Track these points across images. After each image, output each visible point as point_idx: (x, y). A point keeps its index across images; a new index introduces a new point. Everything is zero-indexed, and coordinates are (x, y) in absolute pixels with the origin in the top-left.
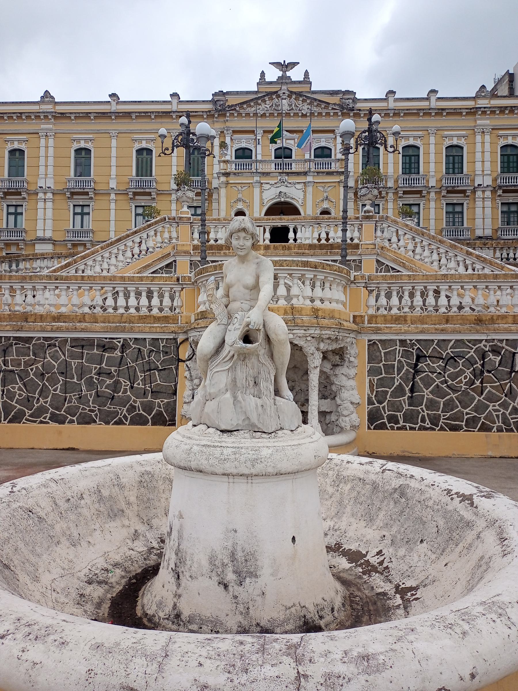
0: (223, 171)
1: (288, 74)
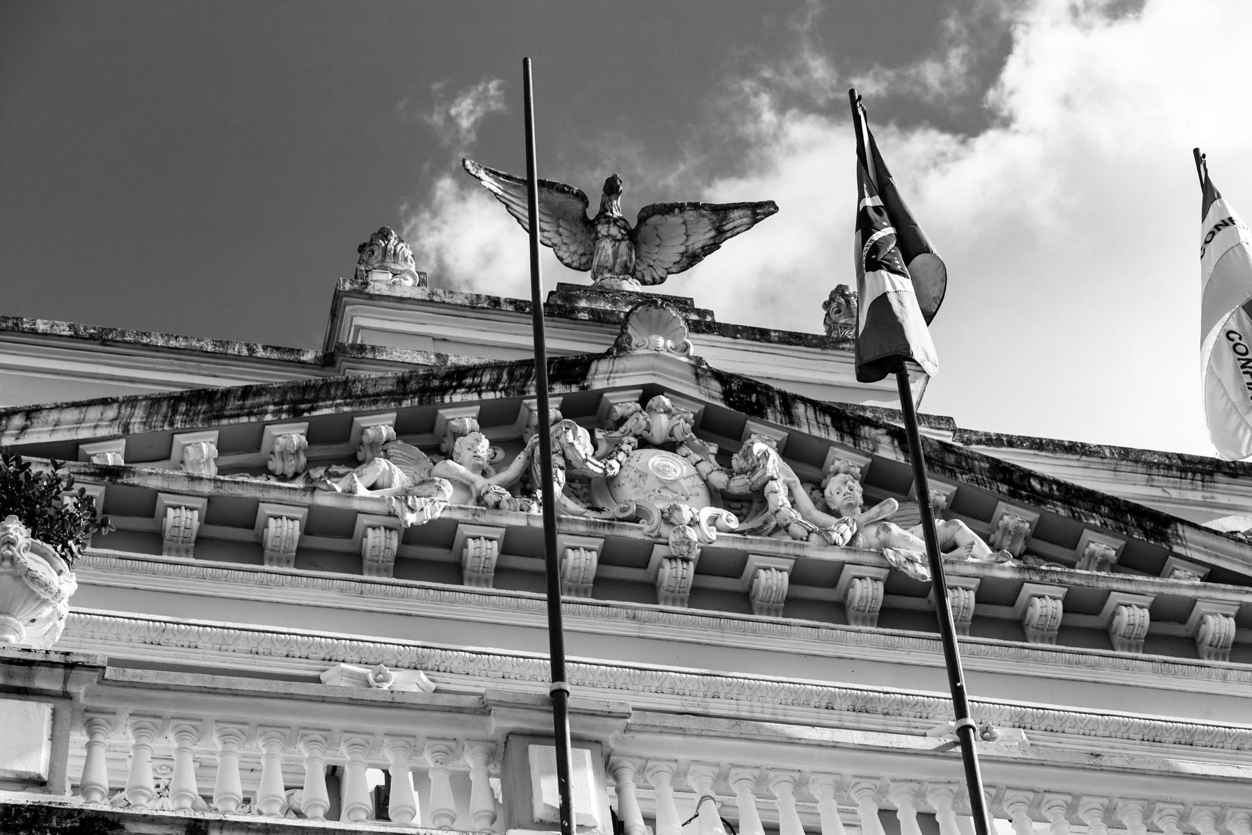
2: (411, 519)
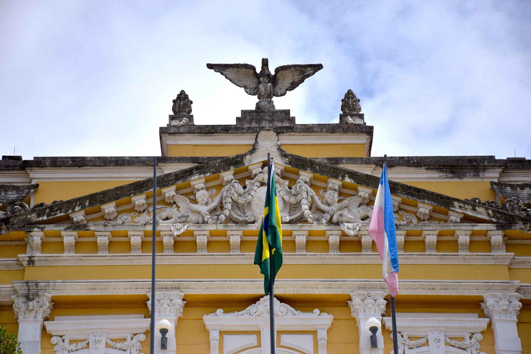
1: (279, 103)
2: (176, 233)
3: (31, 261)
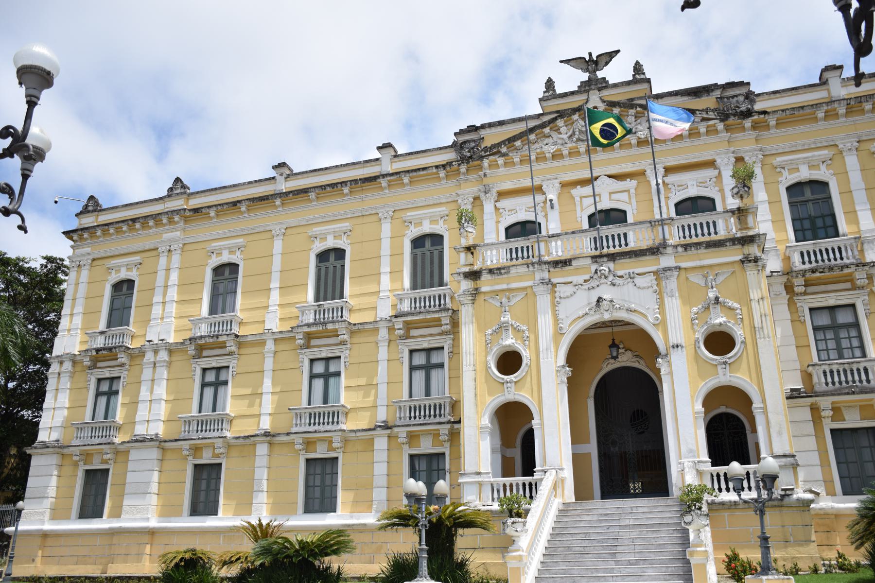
0: (467, 269)
1: (600, 74)
3: (485, 175)
